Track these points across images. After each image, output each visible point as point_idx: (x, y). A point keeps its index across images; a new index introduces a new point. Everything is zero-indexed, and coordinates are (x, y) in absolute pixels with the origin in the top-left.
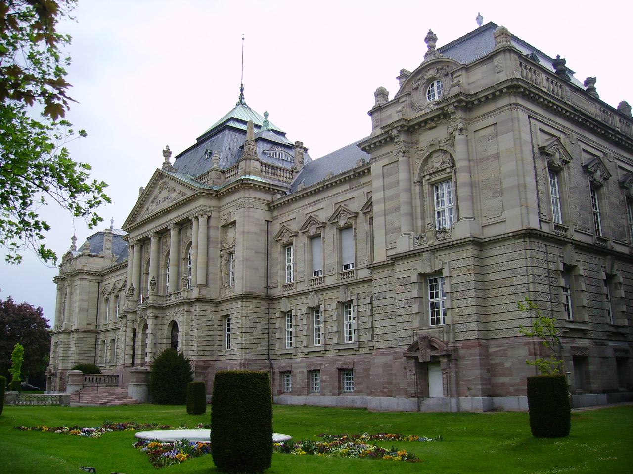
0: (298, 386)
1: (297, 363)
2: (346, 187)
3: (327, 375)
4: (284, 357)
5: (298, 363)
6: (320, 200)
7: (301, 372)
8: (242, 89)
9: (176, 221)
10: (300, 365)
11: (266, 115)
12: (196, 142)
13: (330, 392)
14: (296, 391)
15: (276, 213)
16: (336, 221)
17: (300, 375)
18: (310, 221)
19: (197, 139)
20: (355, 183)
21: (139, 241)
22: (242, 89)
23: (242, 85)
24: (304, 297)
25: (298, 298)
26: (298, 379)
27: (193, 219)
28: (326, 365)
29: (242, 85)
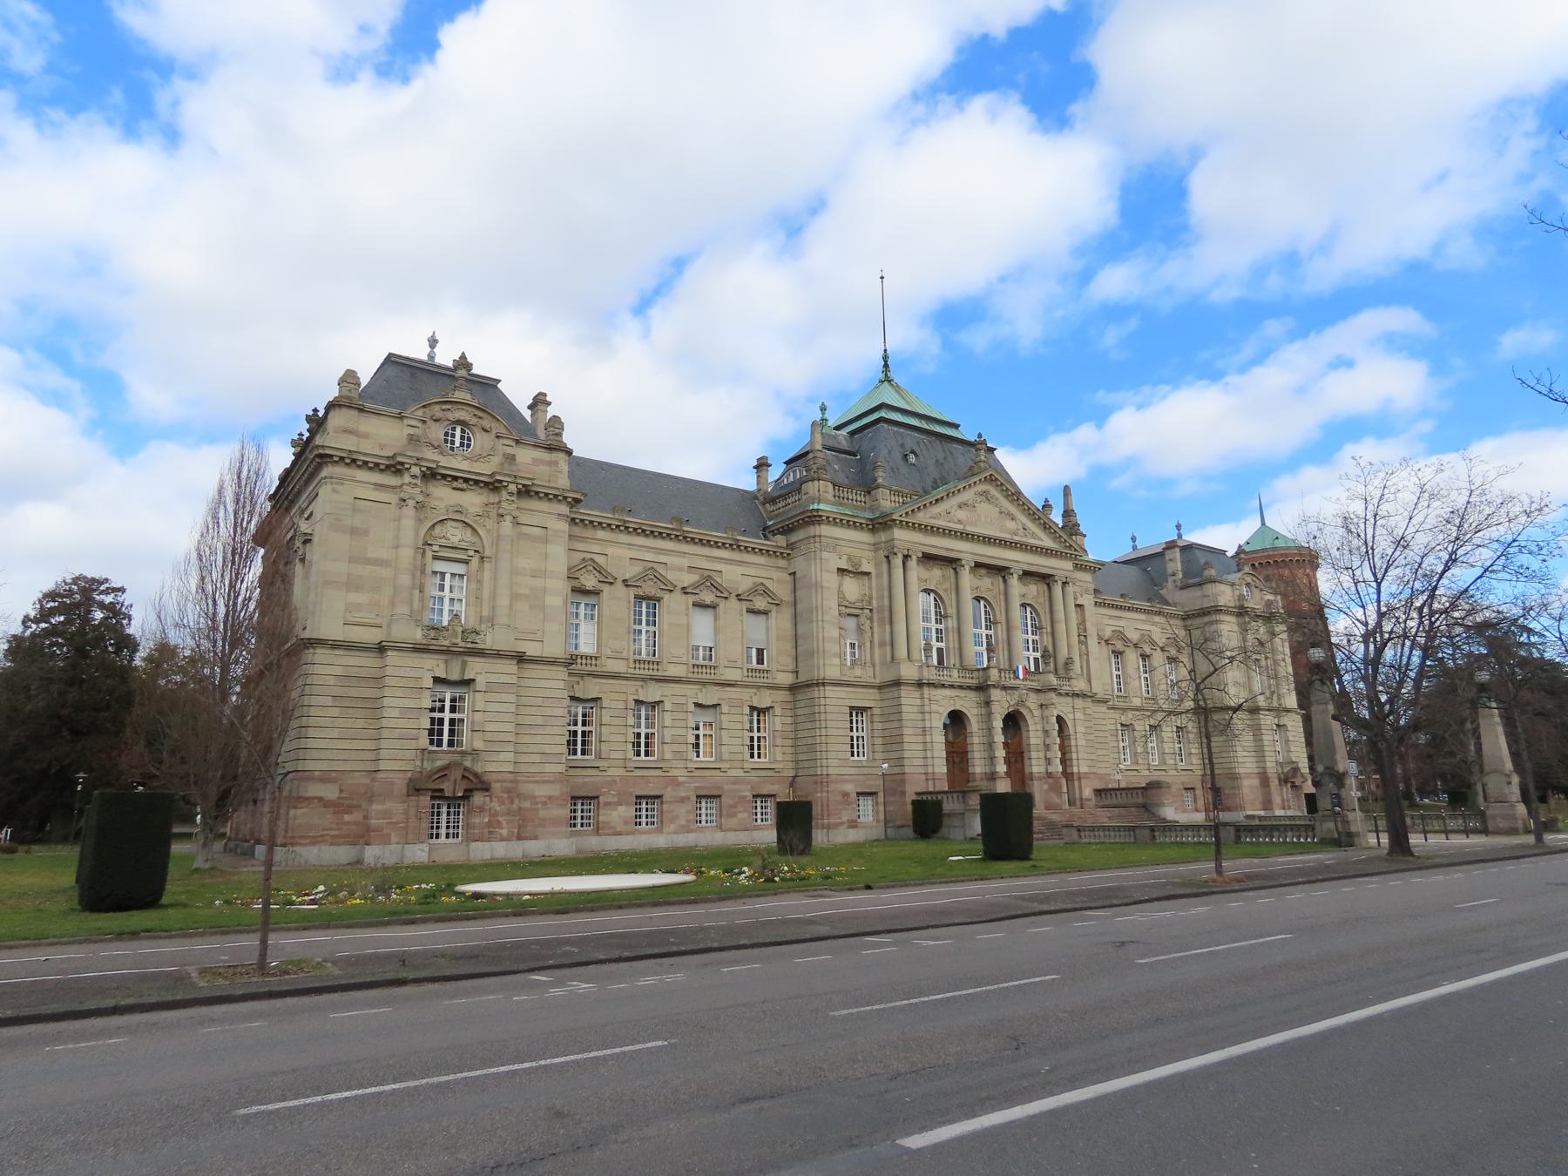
2: (1142, 617)
9: (1026, 568)
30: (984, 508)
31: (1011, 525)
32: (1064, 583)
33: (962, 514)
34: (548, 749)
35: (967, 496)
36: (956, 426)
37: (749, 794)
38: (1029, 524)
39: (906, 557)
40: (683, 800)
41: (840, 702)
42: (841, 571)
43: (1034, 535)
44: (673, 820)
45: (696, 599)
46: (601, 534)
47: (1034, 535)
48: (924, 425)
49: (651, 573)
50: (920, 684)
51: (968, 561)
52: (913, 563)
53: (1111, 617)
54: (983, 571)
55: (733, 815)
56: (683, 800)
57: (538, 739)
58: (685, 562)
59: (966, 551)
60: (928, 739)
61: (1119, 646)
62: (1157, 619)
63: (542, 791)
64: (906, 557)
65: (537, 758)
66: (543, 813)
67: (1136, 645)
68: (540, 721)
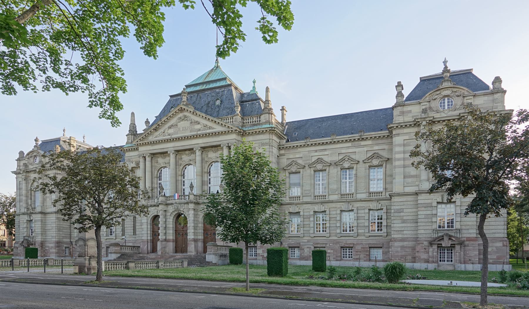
2: (349, 144)
9: (203, 145)
15: (282, 152)
16: (341, 163)
18: (319, 161)
21: (152, 154)
27: (225, 147)
30: (183, 124)
34: (52, 235)
35: (173, 121)
43: (210, 128)
47: (210, 128)
51: (196, 148)
52: (148, 159)
53: (316, 151)
54: (187, 152)
57: (51, 233)
59: (170, 147)
63: (51, 245)
65: (51, 237)
66: (51, 251)
67: (336, 164)
68: (51, 228)
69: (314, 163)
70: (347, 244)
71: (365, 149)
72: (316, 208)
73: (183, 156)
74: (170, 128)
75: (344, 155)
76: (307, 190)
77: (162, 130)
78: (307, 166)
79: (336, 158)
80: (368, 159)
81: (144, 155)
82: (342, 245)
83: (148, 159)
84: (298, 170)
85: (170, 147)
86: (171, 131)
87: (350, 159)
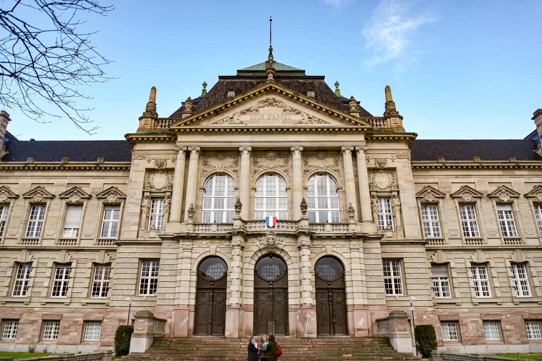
0: (472, 335)
1: (463, 313)
2: (501, 173)
3: (511, 324)
4: (443, 306)
5: (465, 313)
6: (471, 175)
7: (472, 321)
8: (271, 50)
9: (308, 145)
10: (469, 315)
11: (337, 84)
12: (235, 74)
13: (518, 340)
14: (470, 340)
17: (474, 325)
19: (239, 71)
20: (510, 172)
22: (271, 50)
23: (271, 46)
24: (463, 252)
25: (453, 252)
26: (471, 328)
27: (348, 152)
28: (508, 316)
29: (271, 46)
31: (298, 118)
32: (354, 153)
33: (246, 118)
36: (304, 72)
37: (81, 320)
38: (312, 113)
39: (188, 154)
40: (33, 322)
41: (132, 255)
42: (149, 171)
43: (319, 121)
44: (23, 335)
45: (68, 200)
46: (17, 173)
48: (251, 74)
49: (37, 189)
50: (178, 238)
52: (194, 156)
53: (457, 176)
54: (271, 154)
55: (67, 334)
56: (33, 322)
58: (66, 181)
60: (178, 278)
61: (468, 198)
62: (517, 173)
64: (188, 154)
67: (490, 197)
69: (458, 192)
70: (532, 314)
71: (523, 180)
72: (473, 257)
73: (259, 160)
74: (243, 113)
75: (501, 185)
76: (453, 230)
77: (230, 114)
78: (448, 196)
79: (491, 189)
80: (532, 192)
81: (189, 149)
82: (526, 317)
83: (194, 156)
84: (436, 200)
85: (245, 142)
86: (244, 118)
87: (510, 191)
